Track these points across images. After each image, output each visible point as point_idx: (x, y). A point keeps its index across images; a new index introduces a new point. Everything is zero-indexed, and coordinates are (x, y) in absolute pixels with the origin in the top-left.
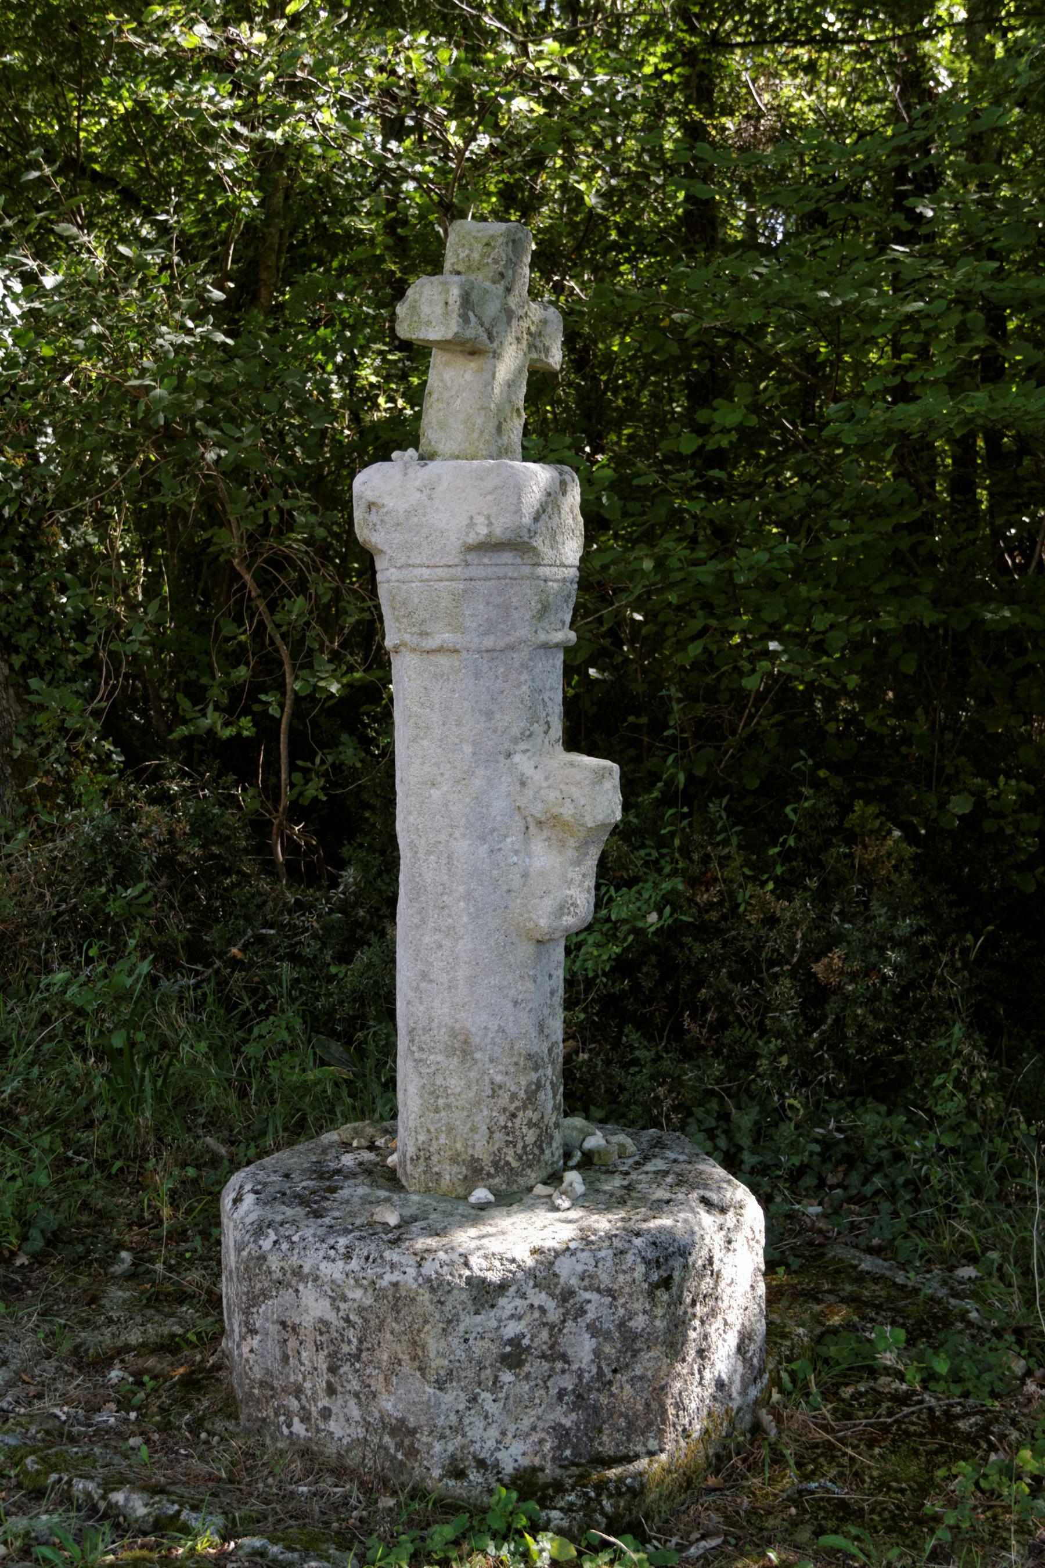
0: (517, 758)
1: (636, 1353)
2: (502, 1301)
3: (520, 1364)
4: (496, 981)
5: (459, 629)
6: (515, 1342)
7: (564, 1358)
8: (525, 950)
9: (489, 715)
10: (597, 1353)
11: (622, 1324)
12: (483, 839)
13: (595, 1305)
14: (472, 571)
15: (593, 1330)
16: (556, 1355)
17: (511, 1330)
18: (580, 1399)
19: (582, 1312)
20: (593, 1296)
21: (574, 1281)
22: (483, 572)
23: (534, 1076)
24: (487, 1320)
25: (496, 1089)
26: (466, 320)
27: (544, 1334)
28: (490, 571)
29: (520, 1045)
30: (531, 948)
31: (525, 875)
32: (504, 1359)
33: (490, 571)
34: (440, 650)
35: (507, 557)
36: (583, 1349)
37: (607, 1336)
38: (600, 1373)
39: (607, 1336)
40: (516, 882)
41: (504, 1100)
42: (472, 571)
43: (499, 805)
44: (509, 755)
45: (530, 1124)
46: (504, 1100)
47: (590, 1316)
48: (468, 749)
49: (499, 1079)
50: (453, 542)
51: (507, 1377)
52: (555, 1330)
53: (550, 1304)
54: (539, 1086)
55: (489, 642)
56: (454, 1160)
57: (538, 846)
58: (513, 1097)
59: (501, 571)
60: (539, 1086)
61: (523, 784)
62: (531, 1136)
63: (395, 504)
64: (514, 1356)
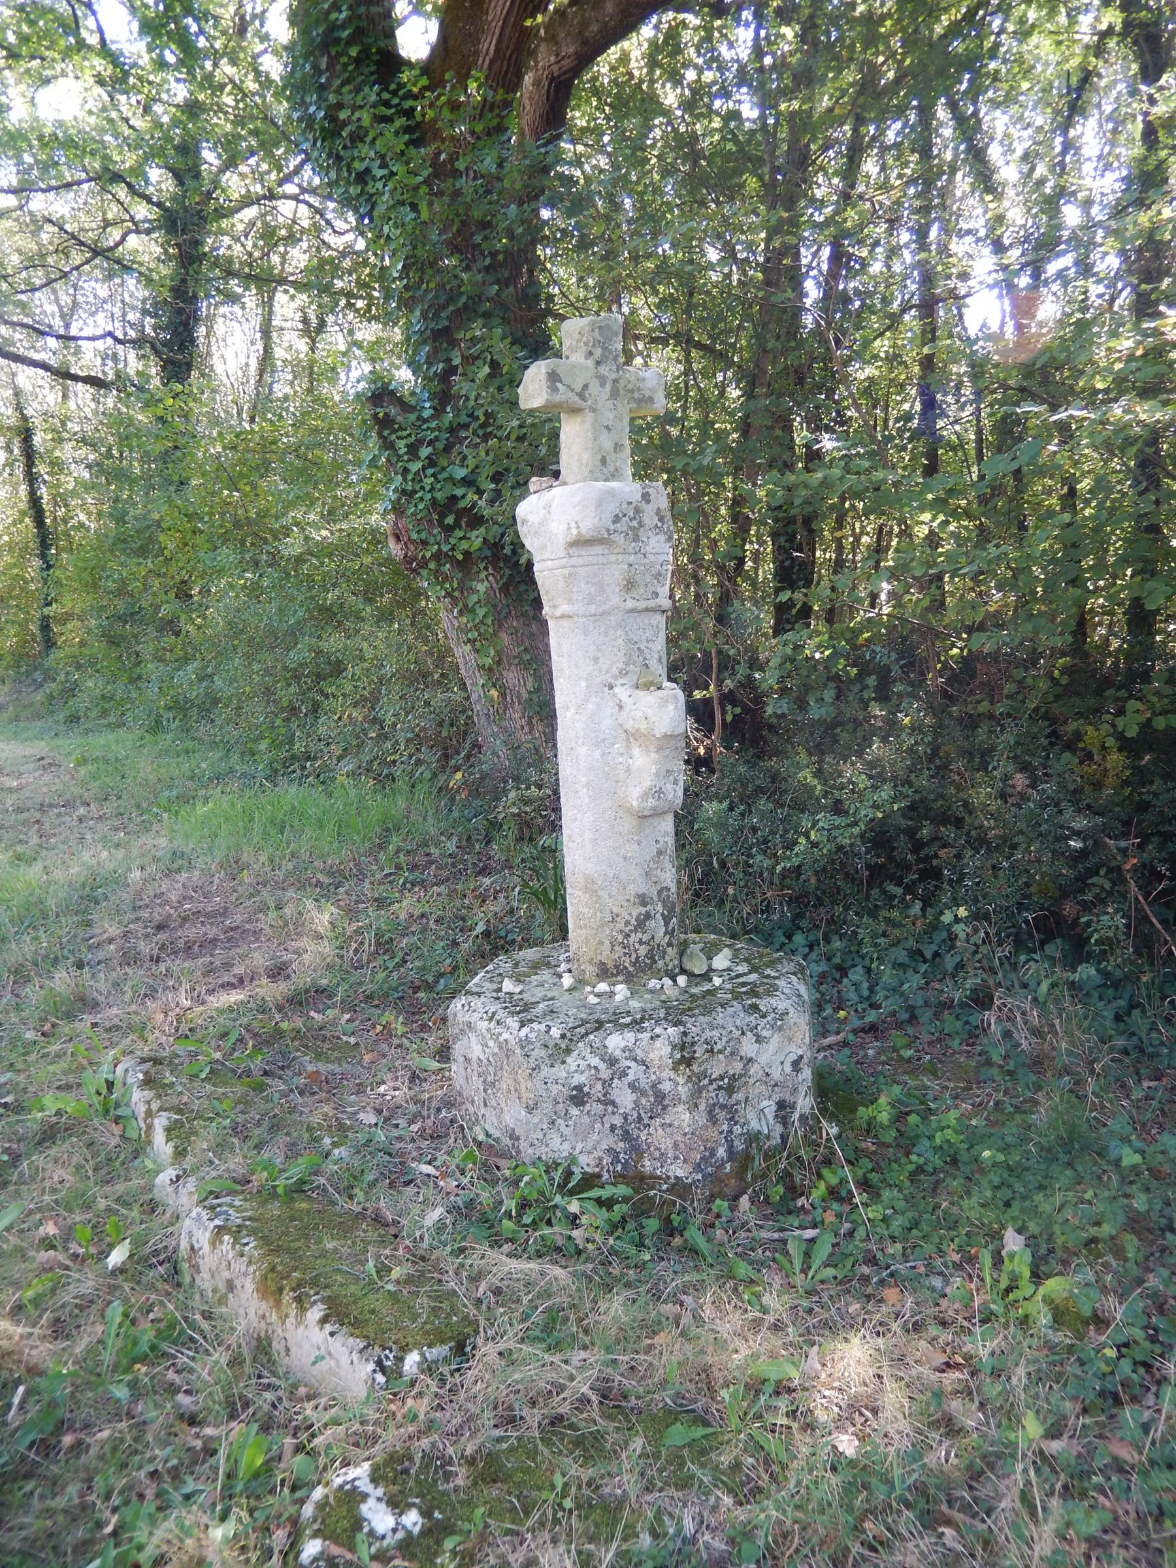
0: (617, 690)
1: (665, 1108)
2: (569, 1060)
3: (583, 1103)
4: (610, 843)
5: (571, 601)
6: (579, 1088)
7: (613, 1103)
8: (628, 824)
9: (596, 660)
10: (637, 1103)
11: (654, 1086)
12: (597, 745)
13: (635, 1071)
14: (574, 561)
15: (633, 1086)
16: (607, 1101)
17: (577, 1079)
18: (626, 1136)
19: (624, 1074)
20: (633, 1064)
21: (618, 1053)
22: (581, 561)
23: (643, 910)
24: (559, 1072)
25: (615, 917)
26: (555, 390)
27: (599, 1086)
28: (594, 560)
29: (633, 889)
30: (635, 822)
31: (628, 770)
32: (572, 1098)
33: (586, 560)
34: (562, 617)
35: (599, 549)
36: (625, 1099)
37: (643, 1093)
38: (640, 1119)
39: (643, 1093)
40: (622, 775)
41: (621, 925)
42: (574, 561)
43: (607, 723)
44: (611, 687)
45: (641, 942)
46: (621, 925)
47: (631, 1078)
48: (583, 684)
49: (616, 910)
50: (561, 541)
51: (574, 1111)
52: (608, 1084)
53: (602, 1066)
54: (648, 916)
55: (592, 609)
56: (591, 961)
57: (636, 751)
58: (627, 923)
59: (594, 560)
60: (648, 916)
61: (621, 707)
62: (643, 950)
63: (534, 519)
64: (579, 1097)
